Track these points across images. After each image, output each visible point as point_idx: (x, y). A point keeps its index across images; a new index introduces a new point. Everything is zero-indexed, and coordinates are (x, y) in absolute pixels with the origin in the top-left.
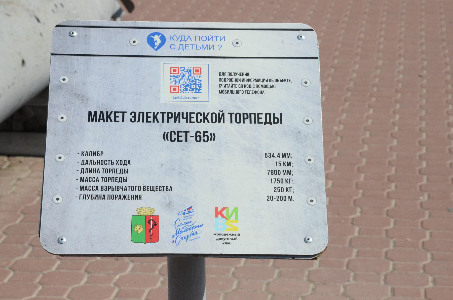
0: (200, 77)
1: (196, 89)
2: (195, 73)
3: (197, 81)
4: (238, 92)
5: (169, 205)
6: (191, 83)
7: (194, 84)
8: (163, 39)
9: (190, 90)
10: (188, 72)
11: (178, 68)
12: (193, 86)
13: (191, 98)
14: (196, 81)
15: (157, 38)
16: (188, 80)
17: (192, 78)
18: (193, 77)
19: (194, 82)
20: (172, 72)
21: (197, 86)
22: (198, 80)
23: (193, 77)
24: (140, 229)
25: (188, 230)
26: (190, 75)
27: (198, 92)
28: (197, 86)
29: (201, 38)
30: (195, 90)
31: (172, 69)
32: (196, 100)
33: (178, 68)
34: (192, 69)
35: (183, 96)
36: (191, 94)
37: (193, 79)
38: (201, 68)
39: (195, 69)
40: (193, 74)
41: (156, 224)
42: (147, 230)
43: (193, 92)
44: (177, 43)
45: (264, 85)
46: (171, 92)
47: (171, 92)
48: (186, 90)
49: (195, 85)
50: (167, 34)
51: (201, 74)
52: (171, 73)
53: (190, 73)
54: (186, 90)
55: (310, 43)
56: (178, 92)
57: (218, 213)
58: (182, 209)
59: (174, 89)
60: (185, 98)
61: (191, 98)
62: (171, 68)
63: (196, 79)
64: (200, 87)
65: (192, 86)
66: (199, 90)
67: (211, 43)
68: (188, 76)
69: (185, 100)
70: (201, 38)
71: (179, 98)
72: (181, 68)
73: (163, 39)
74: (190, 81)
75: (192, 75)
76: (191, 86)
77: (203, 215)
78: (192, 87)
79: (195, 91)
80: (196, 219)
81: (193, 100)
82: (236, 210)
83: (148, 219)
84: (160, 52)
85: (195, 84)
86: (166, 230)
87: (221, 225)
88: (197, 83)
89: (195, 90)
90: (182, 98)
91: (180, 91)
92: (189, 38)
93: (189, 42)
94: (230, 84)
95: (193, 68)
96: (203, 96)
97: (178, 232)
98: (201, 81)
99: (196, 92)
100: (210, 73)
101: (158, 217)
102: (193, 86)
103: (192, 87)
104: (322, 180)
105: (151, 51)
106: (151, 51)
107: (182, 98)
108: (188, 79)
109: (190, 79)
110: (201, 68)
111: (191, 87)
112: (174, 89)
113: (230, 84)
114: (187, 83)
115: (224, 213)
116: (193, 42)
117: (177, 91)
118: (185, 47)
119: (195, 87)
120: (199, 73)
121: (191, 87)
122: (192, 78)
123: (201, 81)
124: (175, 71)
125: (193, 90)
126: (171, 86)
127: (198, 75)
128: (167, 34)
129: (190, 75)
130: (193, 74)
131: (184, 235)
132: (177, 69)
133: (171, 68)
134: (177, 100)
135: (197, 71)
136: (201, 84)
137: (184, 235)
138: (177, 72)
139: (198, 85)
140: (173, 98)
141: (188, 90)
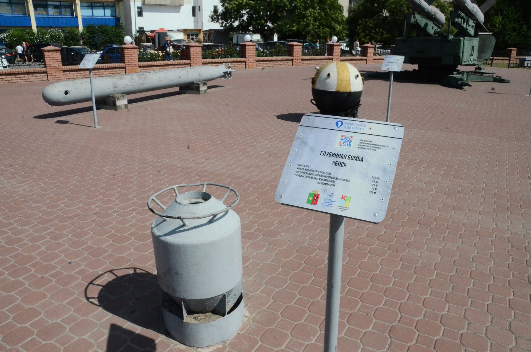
4: (365, 149)
5: (325, 191)
8: (342, 124)
15: (340, 123)
24: (311, 199)
25: (329, 203)
29: (357, 125)
41: (317, 198)
42: (314, 199)
44: (347, 126)
45: (377, 147)
50: (344, 121)
55: (400, 132)
57: (343, 198)
58: (329, 194)
59: (340, 144)
67: (360, 127)
70: (357, 125)
73: (342, 124)
77: (337, 197)
80: (334, 198)
82: (350, 198)
83: (315, 195)
84: (339, 129)
86: (320, 201)
87: (342, 203)
92: (352, 124)
93: (352, 126)
94: (363, 145)
96: (351, 148)
97: (325, 203)
100: (356, 139)
101: (319, 195)
104: (390, 191)
105: (336, 128)
106: (336, 128)
112: (340, 144)
113: (363, 145)
115: (345, 198)
116: (353, 126)
118: (349, 128)
128: (344, 121)
131: (327, 204)
137: (327, 204)
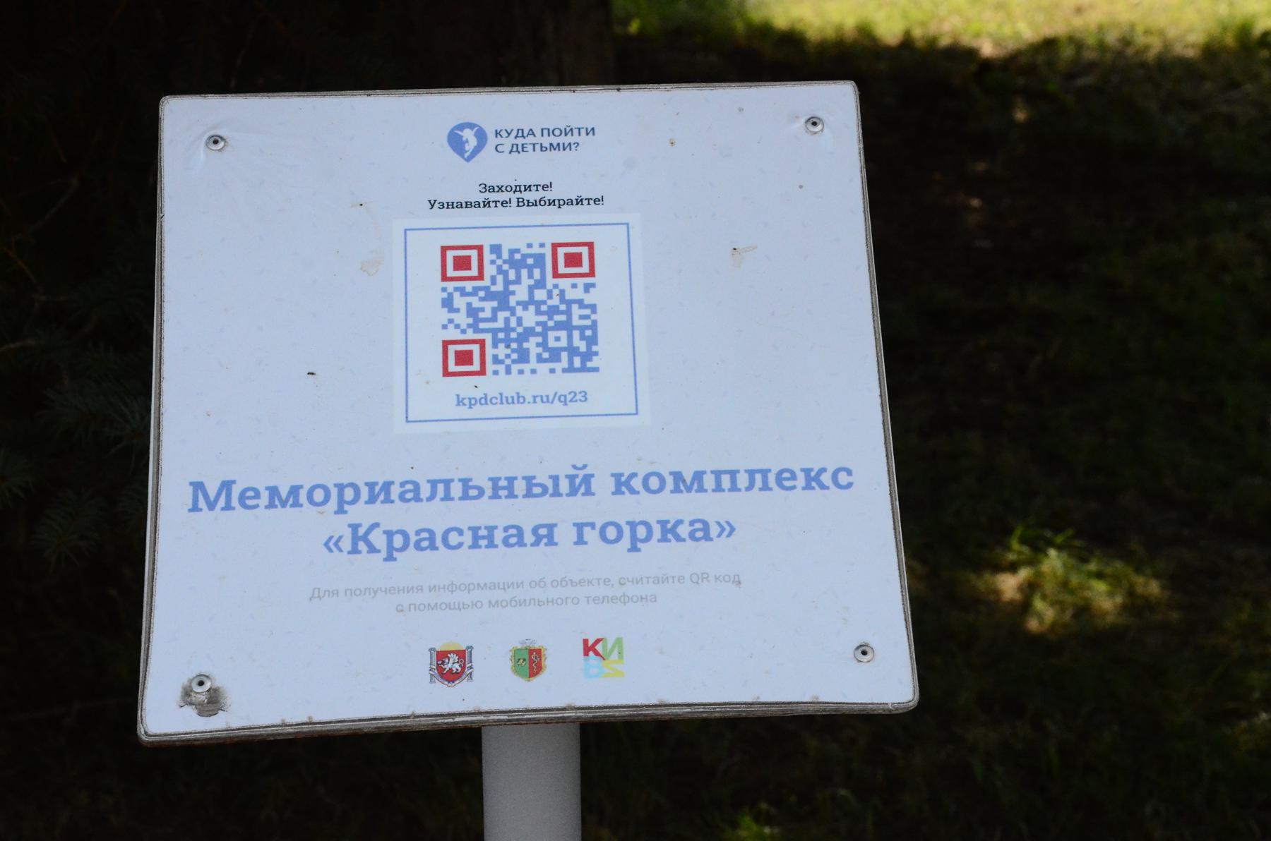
0: (587, 288)
1: (573, 351)
2: (562, 269)
3: (575, 307)
6: (543, 324)
7: (559, 326)
9: (540, 359)
10: (530, 269)
11: (480, 249)
12: (558, 339)
13: (546, 400)
14: (568, 313)
16: (532, 308)
17: (550, 296)
18: (556, 292)
19: (559, 315)
20: (451, 272)
21: (576, 334)
22: (581, 303)
23: (556, 292)
26: (541, 284)
27: (584, 369)
28: (576, 334)
30: (564, 355)
31: (450, 255)
32: (573, 408)
33: (480, 249)
34: (548, 252)
35: (509, 393)
36: (544, 379)
37: (555, 301)
38: (590, 246)
39: (561, 252)
40: (556, 275)
43: (557, 366)
46: (446, 373)
47: (446, 373)
48: (524, 357)
49: (563, 334)
51: (592, 274)
52: (445, 278)
53: (537, 273)
54: (524, 357)
56: (482, 372)
59: (460, 359)
60: (520, 399)
61: (546, 400)
62: (444, 250)
63: (569, 303)
64: (592, 341)
65: (552, 335)
66: (589, 355)
68: (531, 289)
69: (517, 410)
71: (485, 401)
72: (496, 249)
74: (538, 312)
75: (550, 281)
76: (544, 335)
78: (552, 343)
79: (565, 362)
81: (557, 408)
85: (567, 326)
88: (576, 322)
89: (564, 355)
90: (503, 399)
91: (490, 367)
95: (555, 246)
98: (593, 308)
99: (570, 369)
102: (558, 339)
103: (552, 343)
107: (503, 399)
108: (531, 301)
109: (538, 304)
110: (590, 246)
111: (544, 345)
112: (460, 359)
114: (526, 323)
117: (476, 367)
119: (563, 343)
120: (585, 268)
121: (544, 345)
122: (550, 296)
123: (593, 308)
124: (462, 263)
125: (555, 355)
126: (446, 344)
127: (581, 281)
129: (541, 284)
130: (556, 275)
132: (474, 254)
133: (444, 250)
134: (479, 411)
135: (573, 260)
136: (594, 326)
138: (474, 272)
139: (582, 329)
140: (460, 402)
141: (533, 357)
